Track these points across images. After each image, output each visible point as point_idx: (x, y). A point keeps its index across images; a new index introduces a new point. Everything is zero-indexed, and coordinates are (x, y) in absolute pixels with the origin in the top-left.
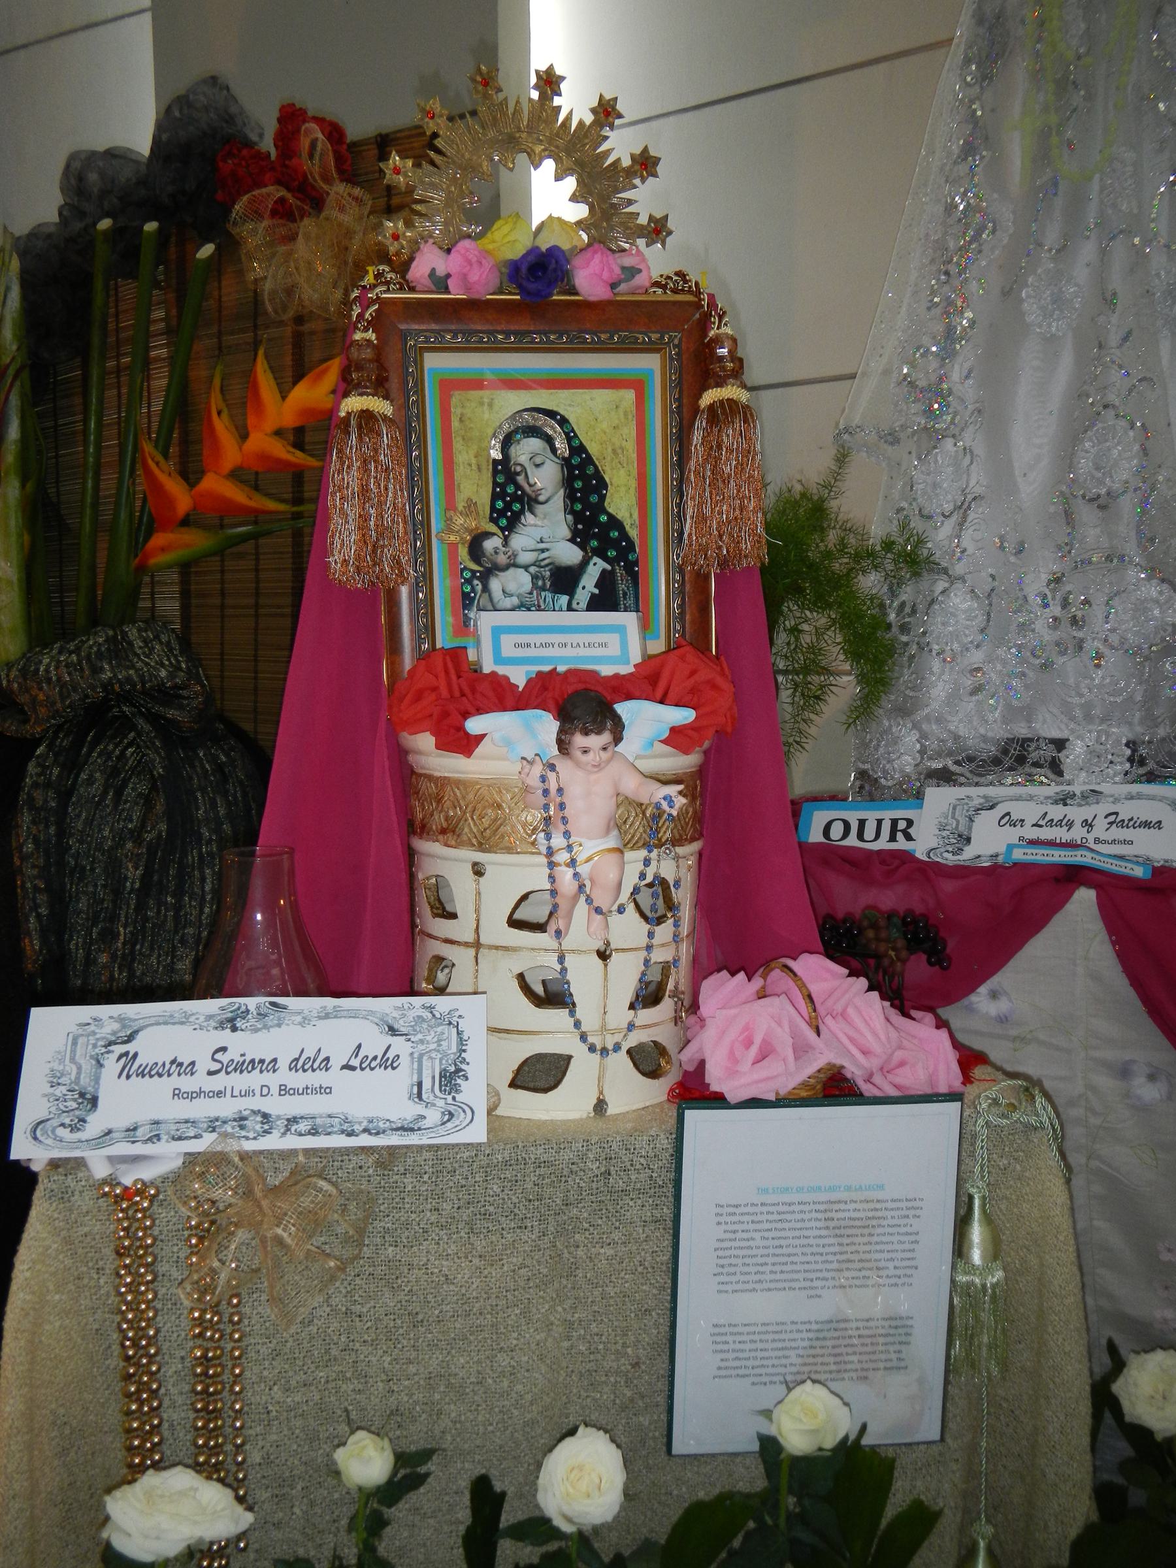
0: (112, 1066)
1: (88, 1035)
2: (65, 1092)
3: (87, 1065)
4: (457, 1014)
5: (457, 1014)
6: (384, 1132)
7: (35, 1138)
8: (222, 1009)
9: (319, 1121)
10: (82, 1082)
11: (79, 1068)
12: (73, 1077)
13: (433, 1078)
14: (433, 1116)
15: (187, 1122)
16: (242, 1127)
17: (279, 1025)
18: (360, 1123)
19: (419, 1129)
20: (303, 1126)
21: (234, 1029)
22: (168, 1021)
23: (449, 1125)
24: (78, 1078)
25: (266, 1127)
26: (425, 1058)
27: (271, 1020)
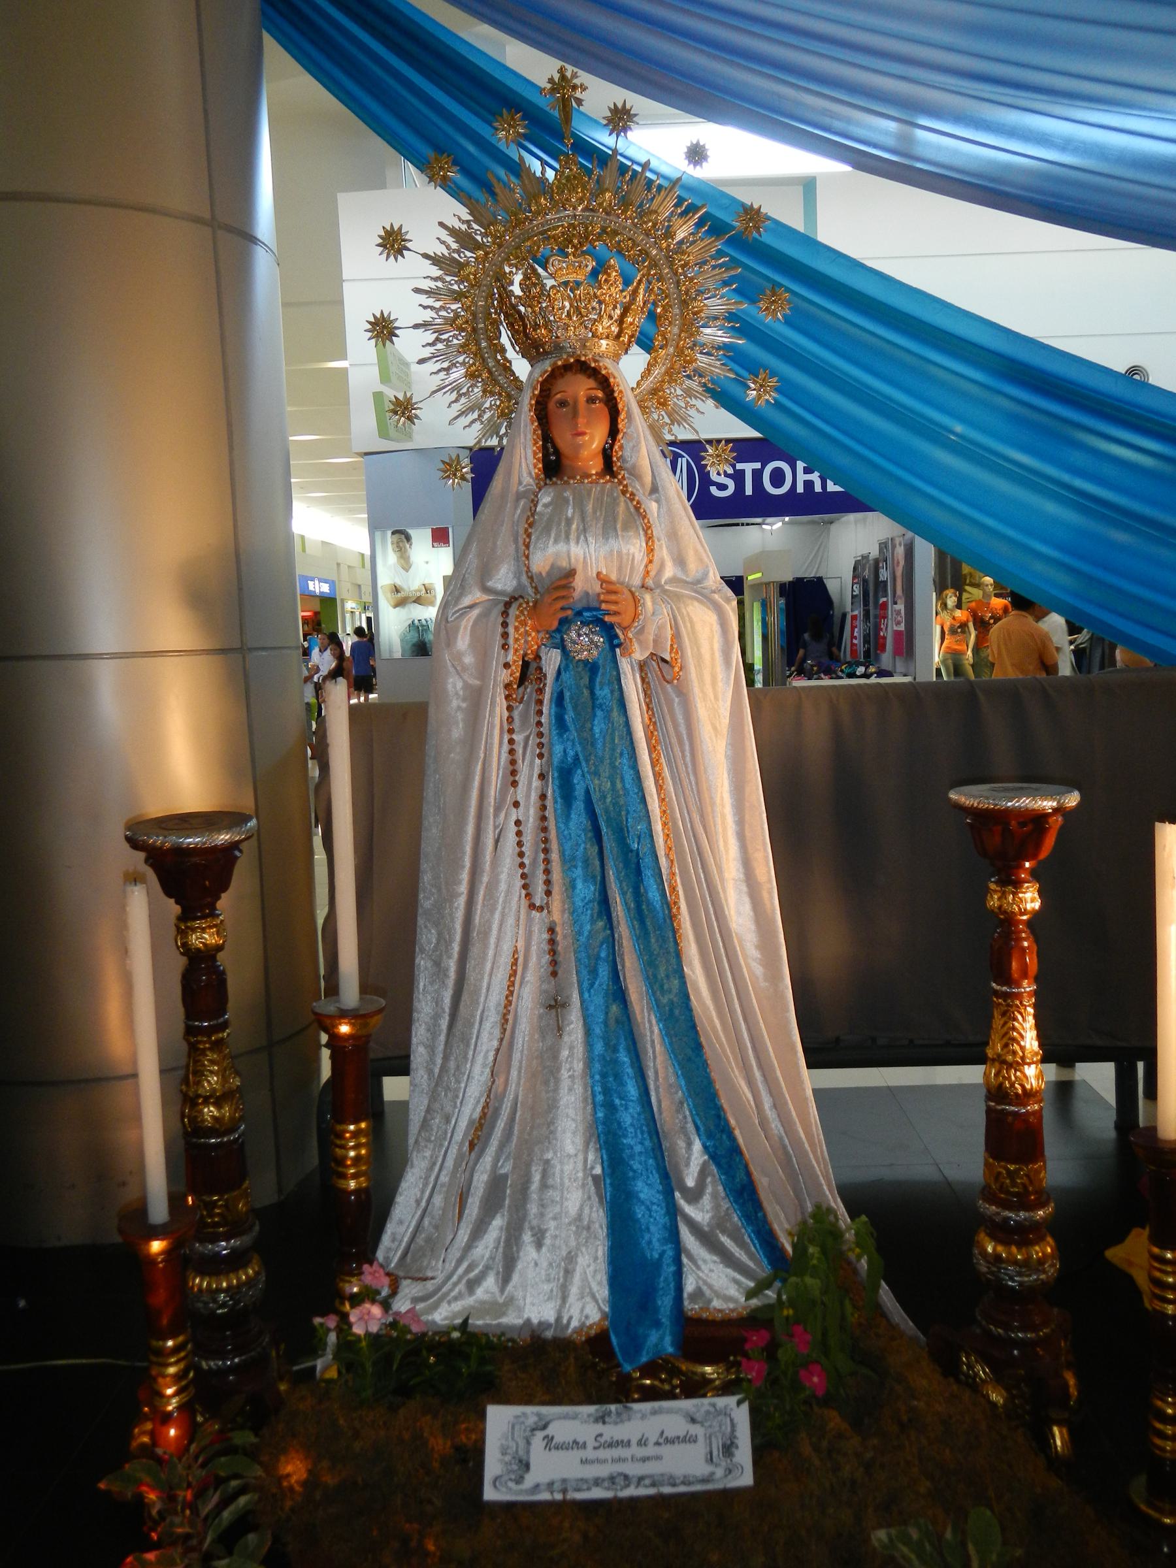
3: (522, 1444)
6: (693, 1483)
9: (656, 1478)
11: (517, 1444)
14: (719, 1472)
15: (582, 1480)
17: (629, 1420)
20: (647, 1482)
21: (604, 1423)
22: (566, 1417)
23: (730, 1477)
24: (517, 1451)
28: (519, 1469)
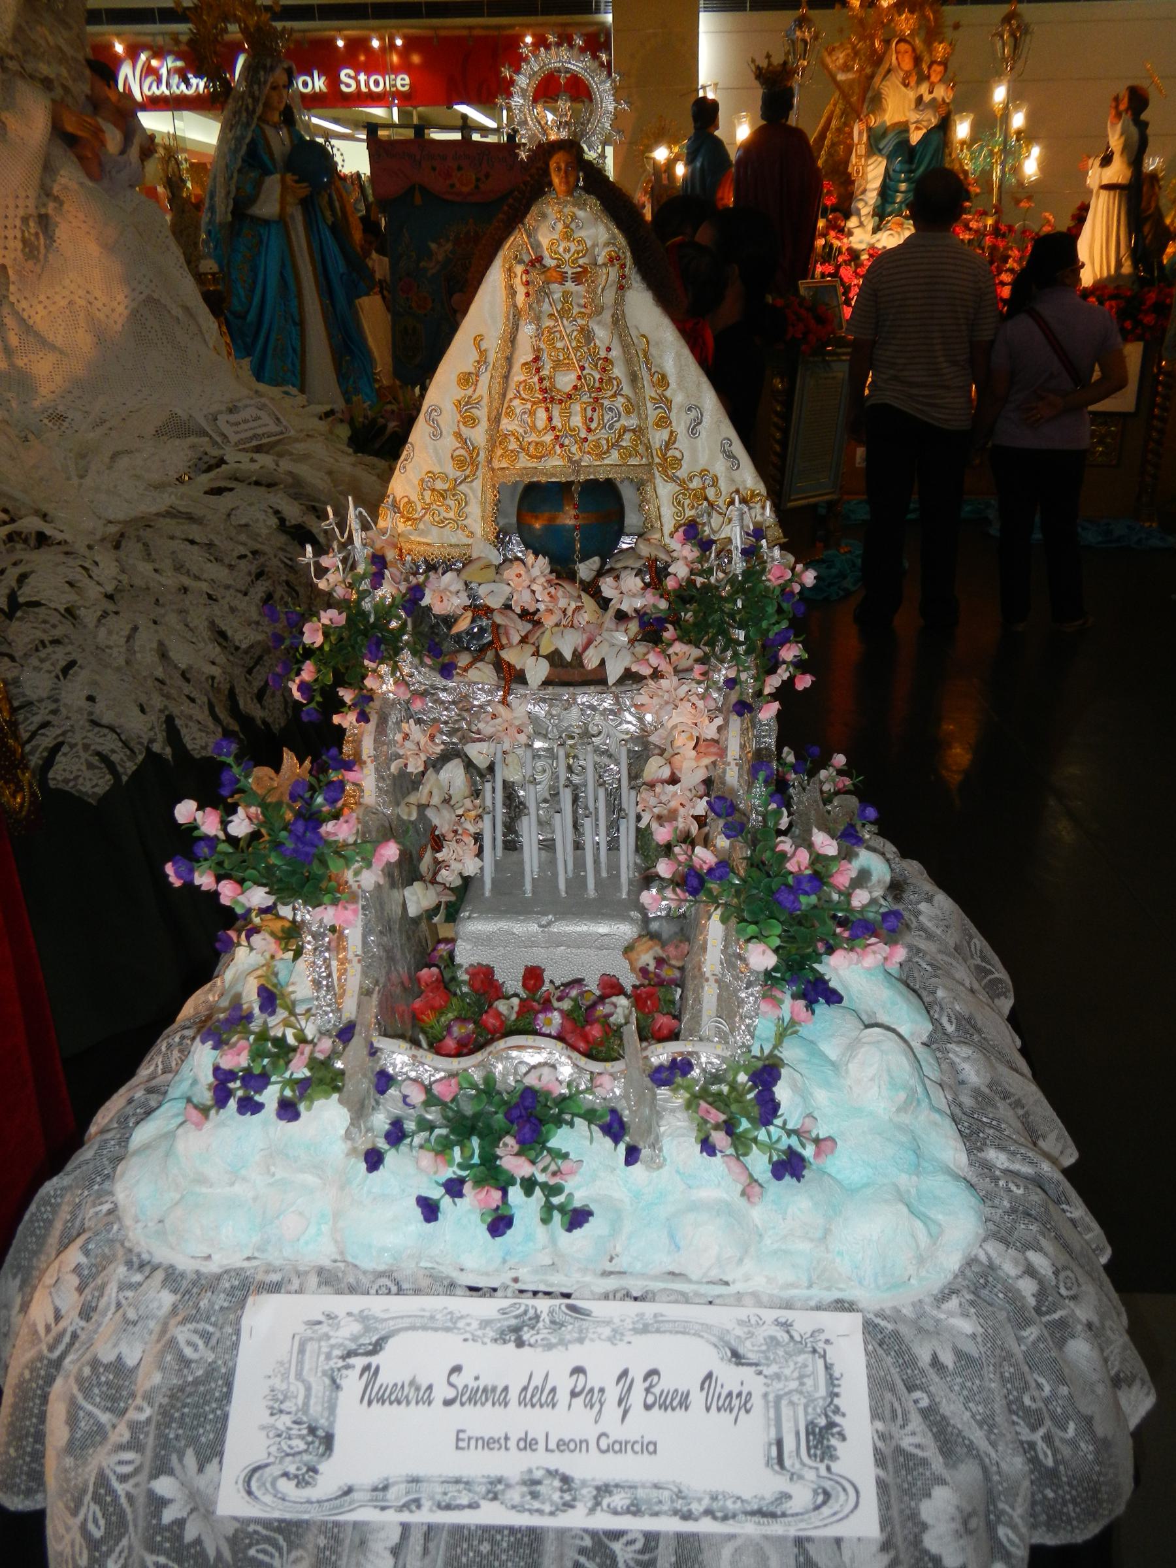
0: (352, 1383)
1: (319, 1340)
2: (289, 1424)
3: (319, 1386)
4: (823, 1337)
5: (823, 1337)
6: (734, 1516)
7: (249, 1493)
8: (503, 1312)
10: (311, 1411)
11: (308, 1389)
12: (300, 1401)
13: (797, 1434)
14: (802, 1497)
15: (457, 1481)
16: (535, 1495)
17: (581, 1341)
18: (700, 1500)
19: (784, 1515)
20: (619, 1500)
21: (520, 1343)
22: (427, 1324)
23: (826, 1511)
24: (306, 1404)
25: (567, 1497)
26: (784, 1402)
27: (569, 1332)
28: (306, 1451)
